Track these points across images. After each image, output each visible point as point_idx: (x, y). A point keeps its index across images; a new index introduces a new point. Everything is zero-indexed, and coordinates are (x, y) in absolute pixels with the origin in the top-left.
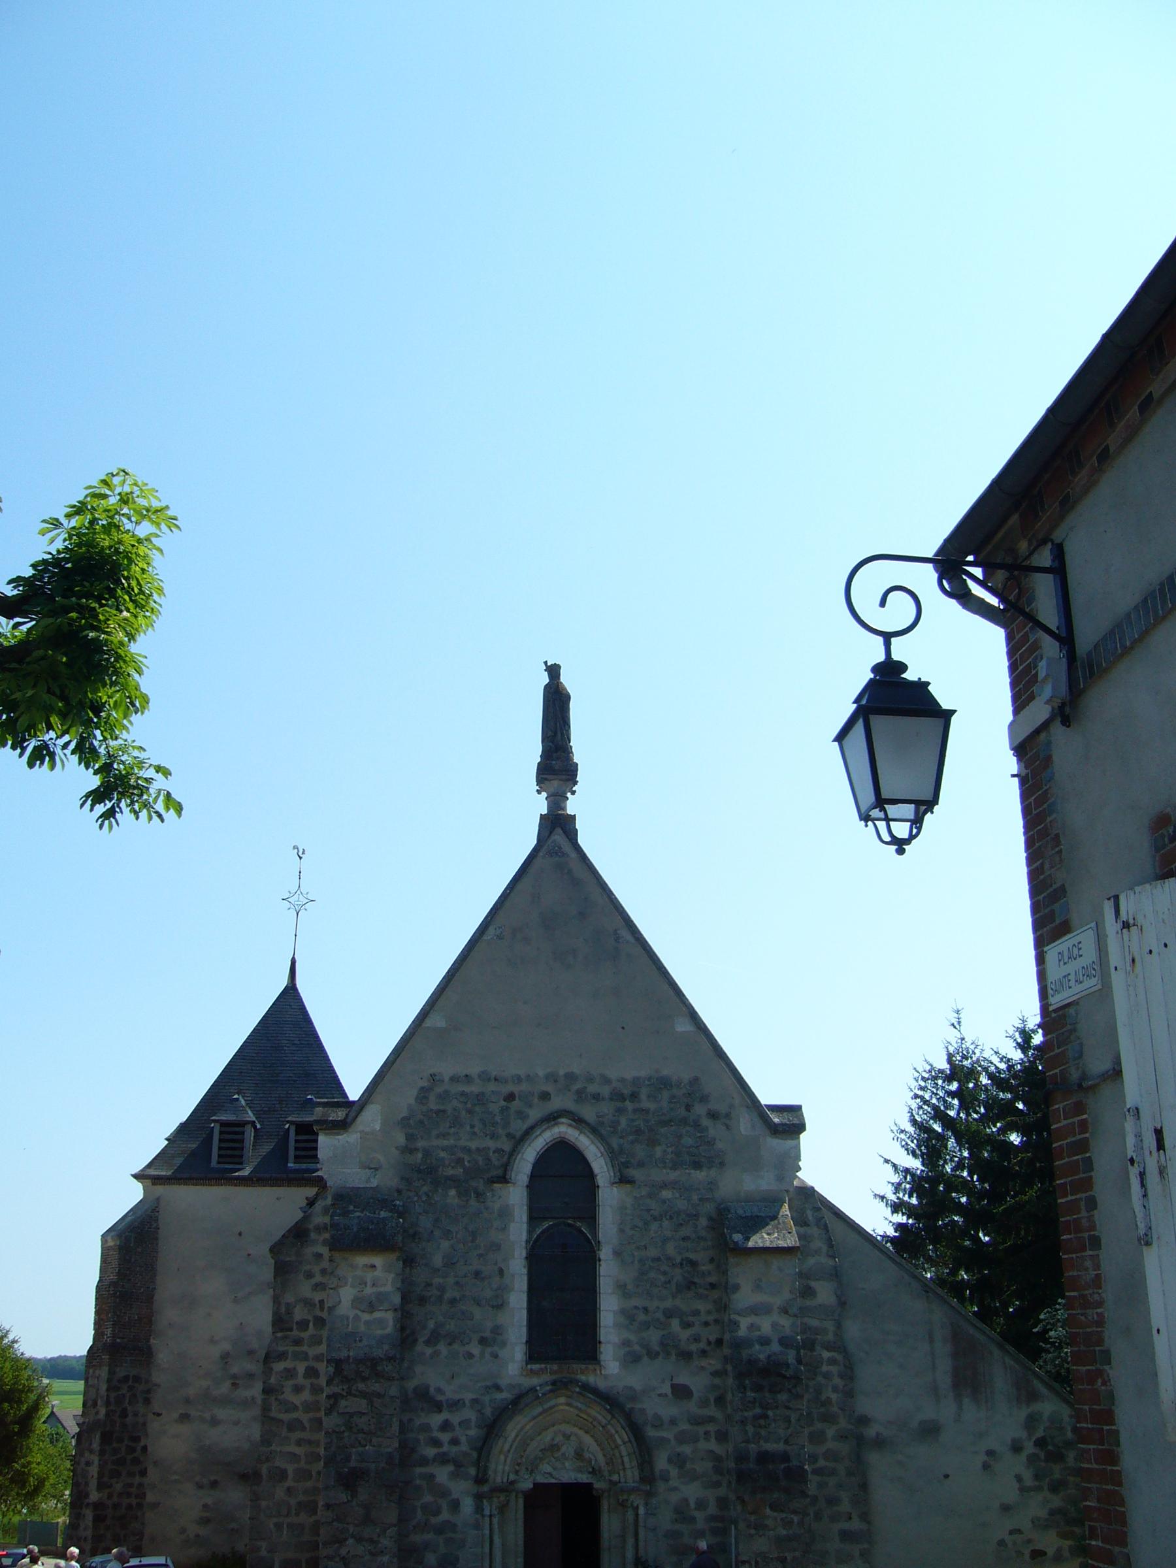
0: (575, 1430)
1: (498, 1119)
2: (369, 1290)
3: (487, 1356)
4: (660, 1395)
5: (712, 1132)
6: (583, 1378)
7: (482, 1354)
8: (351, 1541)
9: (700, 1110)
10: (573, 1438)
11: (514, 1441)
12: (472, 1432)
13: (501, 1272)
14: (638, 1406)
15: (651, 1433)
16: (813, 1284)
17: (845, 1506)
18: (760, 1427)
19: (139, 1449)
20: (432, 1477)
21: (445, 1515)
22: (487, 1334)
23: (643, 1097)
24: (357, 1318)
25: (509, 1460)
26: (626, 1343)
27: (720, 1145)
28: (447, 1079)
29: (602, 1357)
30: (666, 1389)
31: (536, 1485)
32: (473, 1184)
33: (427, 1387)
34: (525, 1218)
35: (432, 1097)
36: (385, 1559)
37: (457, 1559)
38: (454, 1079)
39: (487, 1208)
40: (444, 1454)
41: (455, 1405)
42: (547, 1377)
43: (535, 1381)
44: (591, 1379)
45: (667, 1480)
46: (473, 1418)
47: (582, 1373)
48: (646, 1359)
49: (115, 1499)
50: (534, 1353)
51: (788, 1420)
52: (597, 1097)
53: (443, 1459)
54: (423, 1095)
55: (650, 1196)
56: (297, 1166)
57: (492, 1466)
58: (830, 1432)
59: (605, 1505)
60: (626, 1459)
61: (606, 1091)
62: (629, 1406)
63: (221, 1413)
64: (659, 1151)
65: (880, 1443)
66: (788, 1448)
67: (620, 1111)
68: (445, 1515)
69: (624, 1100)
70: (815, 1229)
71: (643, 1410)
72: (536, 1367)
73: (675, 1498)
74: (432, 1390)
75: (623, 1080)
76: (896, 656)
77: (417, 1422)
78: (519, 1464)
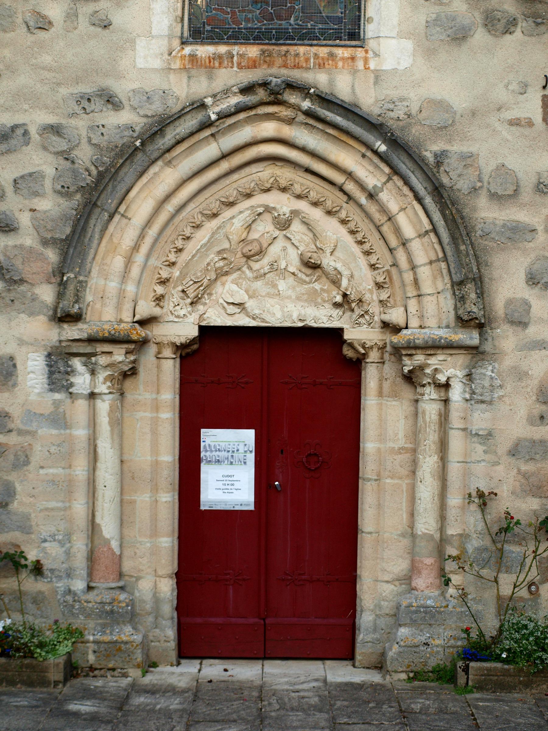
0: (303, 205)
3: (83, 23)
4: (515, 123)
6: (320, 79)
7: (72, 16)
10: (296, 227)
11: (149, 223)
12: (48, 204)
14: (455, 148)
15: (486, 213)
25: (135, 271)
29: (370, 30)
31: (206, 331)
42: (230, 77)
43: (200, 87)
44: (343, 84)
45: (523, 324)
46: (50, 171)
47: (321, 66)
48: (480, 36)
57: (95, 281)
59: (371, 378)
60: (425, 273)
62: (436, 147)
71: (468, 159)
72: (205, 51)
78: (164, 282)
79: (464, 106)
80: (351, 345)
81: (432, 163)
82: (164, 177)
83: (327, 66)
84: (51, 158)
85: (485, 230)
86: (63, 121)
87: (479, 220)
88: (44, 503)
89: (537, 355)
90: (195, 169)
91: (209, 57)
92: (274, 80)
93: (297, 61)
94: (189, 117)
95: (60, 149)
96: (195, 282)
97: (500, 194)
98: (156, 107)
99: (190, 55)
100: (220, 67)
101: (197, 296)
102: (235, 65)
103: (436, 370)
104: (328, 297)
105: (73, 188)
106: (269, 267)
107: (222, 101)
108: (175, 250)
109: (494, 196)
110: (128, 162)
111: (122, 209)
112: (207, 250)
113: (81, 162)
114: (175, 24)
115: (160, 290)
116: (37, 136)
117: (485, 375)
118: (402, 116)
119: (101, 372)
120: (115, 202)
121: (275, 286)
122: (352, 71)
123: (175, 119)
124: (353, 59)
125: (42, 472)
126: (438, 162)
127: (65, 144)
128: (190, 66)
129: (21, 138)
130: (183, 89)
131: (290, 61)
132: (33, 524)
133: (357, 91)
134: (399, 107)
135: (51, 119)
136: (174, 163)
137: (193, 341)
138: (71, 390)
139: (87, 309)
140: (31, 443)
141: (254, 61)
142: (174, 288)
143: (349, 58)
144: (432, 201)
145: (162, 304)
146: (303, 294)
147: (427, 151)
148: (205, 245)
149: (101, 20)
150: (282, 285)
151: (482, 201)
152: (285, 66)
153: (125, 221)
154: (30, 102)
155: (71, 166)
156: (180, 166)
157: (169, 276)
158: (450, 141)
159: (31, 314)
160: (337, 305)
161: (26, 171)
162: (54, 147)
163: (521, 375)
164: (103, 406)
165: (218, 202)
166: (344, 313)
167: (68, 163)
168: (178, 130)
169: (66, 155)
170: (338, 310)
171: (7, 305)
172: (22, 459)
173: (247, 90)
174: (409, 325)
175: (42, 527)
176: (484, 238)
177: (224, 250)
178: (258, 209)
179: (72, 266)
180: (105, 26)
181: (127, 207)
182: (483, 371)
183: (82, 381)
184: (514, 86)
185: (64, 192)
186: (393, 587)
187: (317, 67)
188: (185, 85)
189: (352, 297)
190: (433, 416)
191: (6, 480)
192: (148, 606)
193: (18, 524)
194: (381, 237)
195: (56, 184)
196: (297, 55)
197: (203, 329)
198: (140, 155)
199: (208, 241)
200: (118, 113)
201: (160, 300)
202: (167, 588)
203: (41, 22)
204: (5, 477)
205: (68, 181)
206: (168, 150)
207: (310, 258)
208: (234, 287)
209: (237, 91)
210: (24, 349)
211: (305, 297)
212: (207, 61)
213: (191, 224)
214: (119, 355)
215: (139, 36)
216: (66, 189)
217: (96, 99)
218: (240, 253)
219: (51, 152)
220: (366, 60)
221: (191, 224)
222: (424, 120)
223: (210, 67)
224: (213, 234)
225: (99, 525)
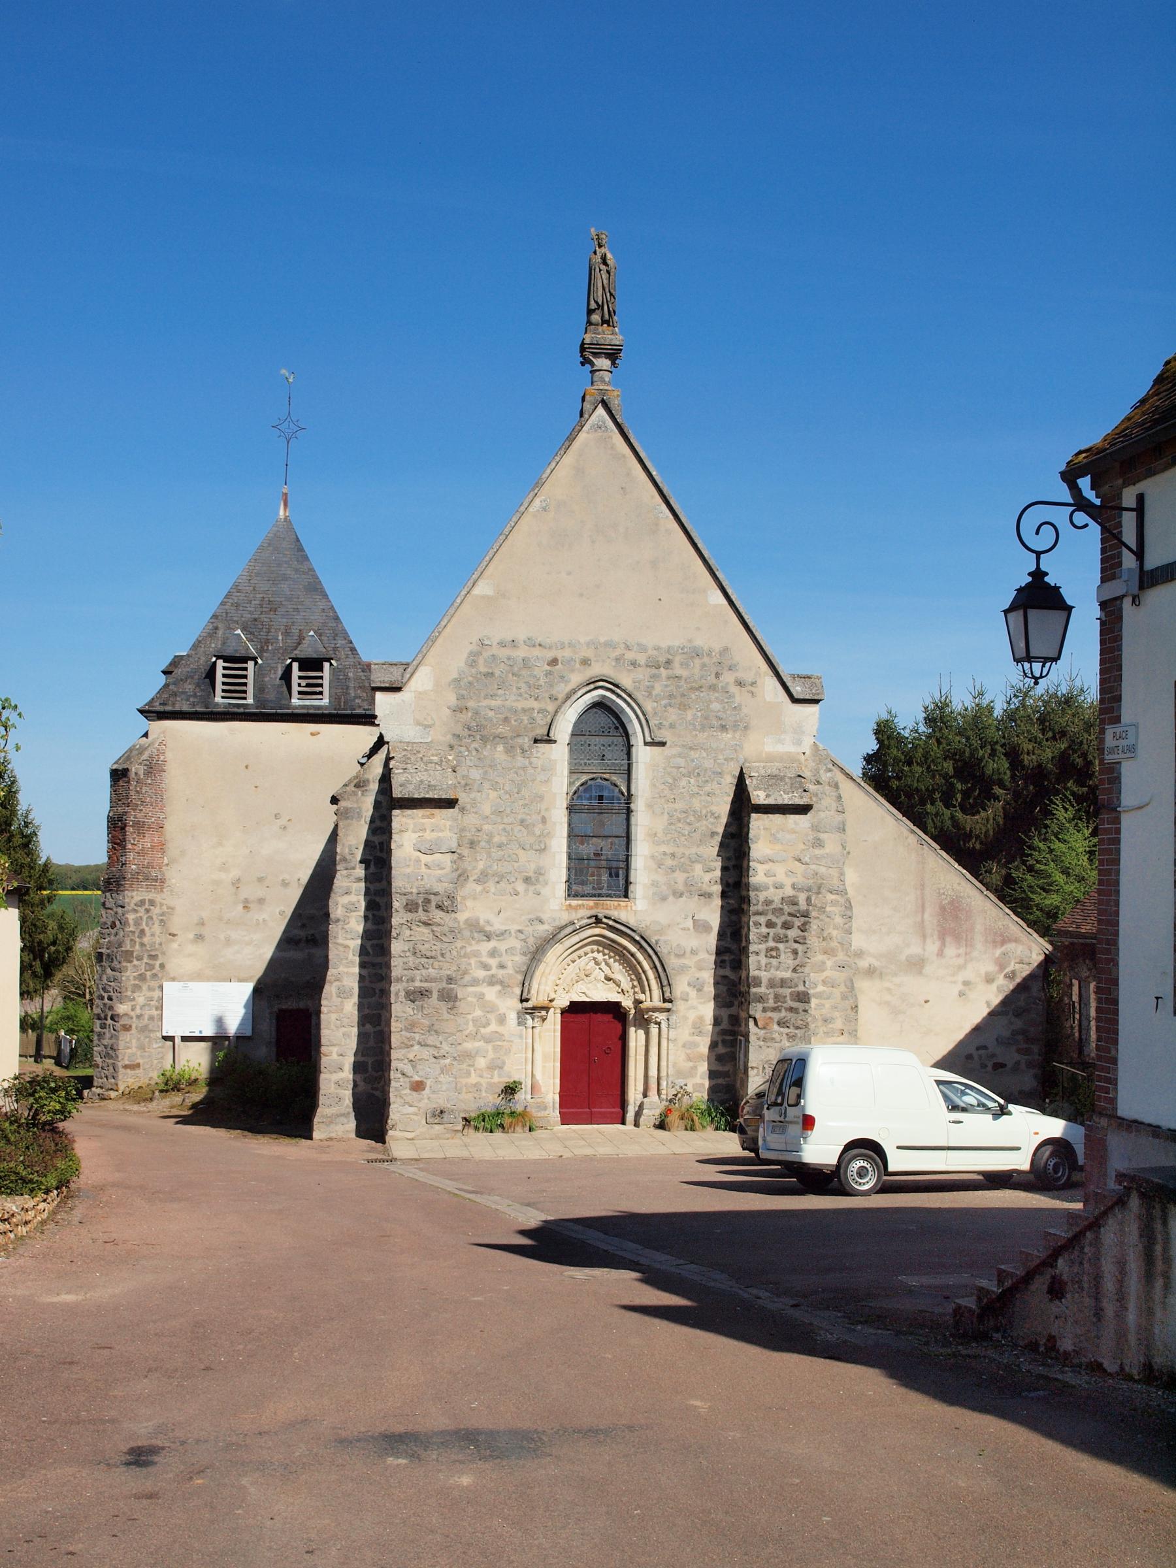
1: (542, 682)
2: (428, 835)
3: (530, 894)
4: (683, 929)
5: (738, 699)
6: (614, 914)
7: (526, 891)
8: (417, 1047)
9: (728, 678)
12: (520, 960)
13: (544, 820)
15: (672, 962)
16: (823, 836)
17: (839, 1024)
18: (772, 957)
19: (157, 966)
20: (481, 996)
21: (493, 1027)
22: (531, 874)
23: (676, 664)
24: (418, 861)
26: (654, 884)
27: (745, 710)
28: (495, 644)
32: (520, 741)
33: (477, 920)
34: (566, 772)
35: (481, 661)
36: (447, 1061)
37: (504, 1063)
38: (502, 644)
39: (530, 763)
40: (493, 976)
41: (502, 935)
43: (574, 916)
44: (623, 916)
48: (671, 898)
49: (138, 1011)
50: (571, 894)
51: (795, 952)
52: (634, 664)
53: (492, 981)
54: (472, 664)
55: (680, 755)
56: (301, 703)
57: (535, 986)
58: (829, 964)
61: (642, 659)
63: (234, 935)
64: (689, 715)
65: (871, 972)
66: (795, 975)
67: (654, 677)
68: (493, 1027)
69: (658, 667)
70: (827, 787)
72: (574, 902)
73: (692, 1016)
74: (482, 922)
75: (657, 648)
76: (1043, 568)
77: (469, 949)
82: (558, 949)
98: (558, 924)
130: (565, 917)
151: (672, 957)
163: (685, 1018)
164: (536, 1031)
169: (524, 941)
183: (530, 1022)
185: (524, 954)
202: (557, 1098)
205: (525, 950)
214: (544, 1013)
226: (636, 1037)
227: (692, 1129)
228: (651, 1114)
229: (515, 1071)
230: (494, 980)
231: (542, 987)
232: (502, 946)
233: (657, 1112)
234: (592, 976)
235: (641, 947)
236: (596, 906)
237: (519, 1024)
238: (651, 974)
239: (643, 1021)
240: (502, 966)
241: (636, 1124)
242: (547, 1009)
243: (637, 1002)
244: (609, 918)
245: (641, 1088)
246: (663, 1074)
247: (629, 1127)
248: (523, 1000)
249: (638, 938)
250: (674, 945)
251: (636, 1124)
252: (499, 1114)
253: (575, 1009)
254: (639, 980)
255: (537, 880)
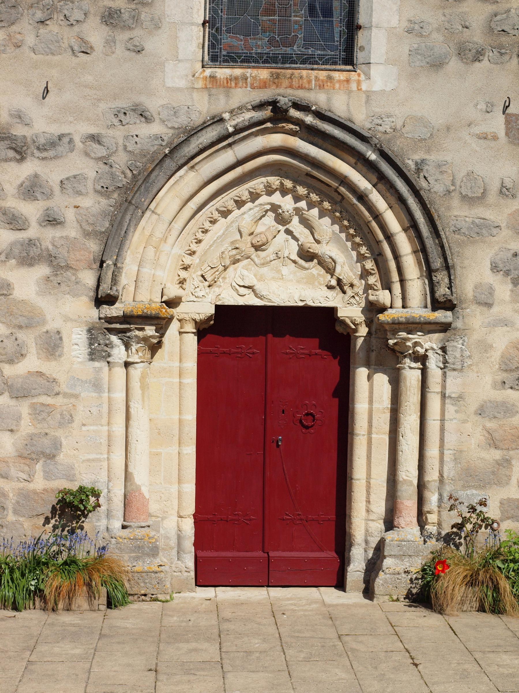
6: (319, 99)
7: (110, 42)
14: (433, 157)
21: (32, 362)
30: (497, 124)
37: (57, 445)
40: (31, 242)
41: (51, 147)
42: (243, 96)
45: (489, 305)
46: (91, 174)
47: (321, 87)
48: (454, 64)
62: (417, 157)
68: (32, 362)
72: (223, 73)
78: (186, 268)
79: (440, 122)
80: (343, 322)
81: (414, 170)
82: (187, 180)
83: (326, 87)
84: (92, 163)
85: (457, 226)
86: (103, 132)
87: (453, 217)
88: (86, 455)
89: (500, 330)
90: (214, 173)
91: (227, 78)
92: (282, 98)
93: (301, 83)
94: (209, 129)
95: (100, 155)
96: (212, 268)
97: (470, 196)
98: (182, 120)
99: (210, 76)
100: (236, 87)
101: (214, 280)
102: (249, 85)
103: (416, 343)
104: (324, 280)
105: (111, 188)
106: (274, 255)
107: (238, 116)
108: (196, 241)
109: (464, 198)
110: (158, 166)
111: (152, 206)
112: (222, 241)
113: (118, 166)
114: (197, 50)
115: (184, 274)
116: (80, 144)
117: (456, 347)
118: (388, 130)
119: (134, 344)
120: (147, 200)
121: (279, 271)
122: (347, 91)
123: (198, 131)
124: (348, 81)
125: (84, 428)
126: (418, 169)
127: (104, 151)
128: (211, 86)
129: (67, 146)
131: (295, 83)
132: (77, 472)
133: (351, 108)
134: (386, 123)
135: (93, 130)
136: (197, 168)
137: (209, 318)
138: (109, 359)
139: (123, 291)
140: (75, 404)
141: (265, 82)
142: (194, 273)
143: (344, 81)
144: (413, 202)
145: (184, 286)
146: (303, 278)
147: (409, 159)
148: (221, 236)
149: (135, 46)
150: (285, 271)
151: (456, 202)
152: (291, 87)
153: (155, 217)
154: (75, 115)
155: (110, 170)
156: (202, 170)
157: (190, 263)
158: (429, 151)
159: (76, 296)
160: (330, 287)
161: (71, 174)
162: (95, 153)
163: (486, 347)
165: (232, 200)
166: (337, 295)
167: (107, 168)
168: (200, 140)
169: (105, 161)
170: (332, 292)
171: (54, 287)
172: (67, 418)
173: (260, 106)
174: (393, 306)
175: (84, 475)
176: (456, 233)
177: (236, 241)
178: (266, 206)
179: (110, 254)
180: (139, 51)
181: (157, 205)
182: (455, 344)
184: (482, 106)
185: (104, 192)
186: (378, 525)
187: (318, 88)
188: (206, 102)
189: (345, 281)
190: (412, 381)
191: (53, 436)
192: (172, 542)
193: (63, 472)
194: (369, 231)
195: (96, 185)
196: (301, 77)
197: (218, 308)
198: (168, 161)
199: (223, 234)
200: (149, 125)
201: (183, 284)
202: (189, 527)
203: (84, 46)
204: (53, 433)
205: (106, 182)
206: (193, 158)
207: (309, 248)
208: (245, 272)
209: (250, 107)
210: (69, 324)
211: (305, 280)
212: (225, 82)
213: (210, 219)
214: (150, 331)
215: (167, 60)
216: (105, 189)
217: (131, 113)
218: (250, 243)
219: (92, 158)
220: (359, 82)
221: (210, 219)
222: (407, 133)
223: (227, 87)
224: (228, 227)
225: (131, 473)
226: (370, 391)
227: (496, 608)
228: (400, 569)
229: (84, 464)
230: (34, 252)
231: (146, 271)
232: (53, 173)
233: (415, 565)
234: (271, 250)
235: (381, 180)
236: (276, 79)
237: (93, 356)
238: (404, 243)
239: (387, 356)
240: (52, 221)
241: (369, 592)
242: (161, 323)
243: (373, 309)
244: (305, 108)
245: (380, 508)
246: (432, 475)
247: (353, 596)
248: (102, 300)
249: (373, 156)
250: (461, 175)
251: (369, 592)
252: (37, 564)
253: (227, 326)
254: (378, 257)
255: (136, 18)
